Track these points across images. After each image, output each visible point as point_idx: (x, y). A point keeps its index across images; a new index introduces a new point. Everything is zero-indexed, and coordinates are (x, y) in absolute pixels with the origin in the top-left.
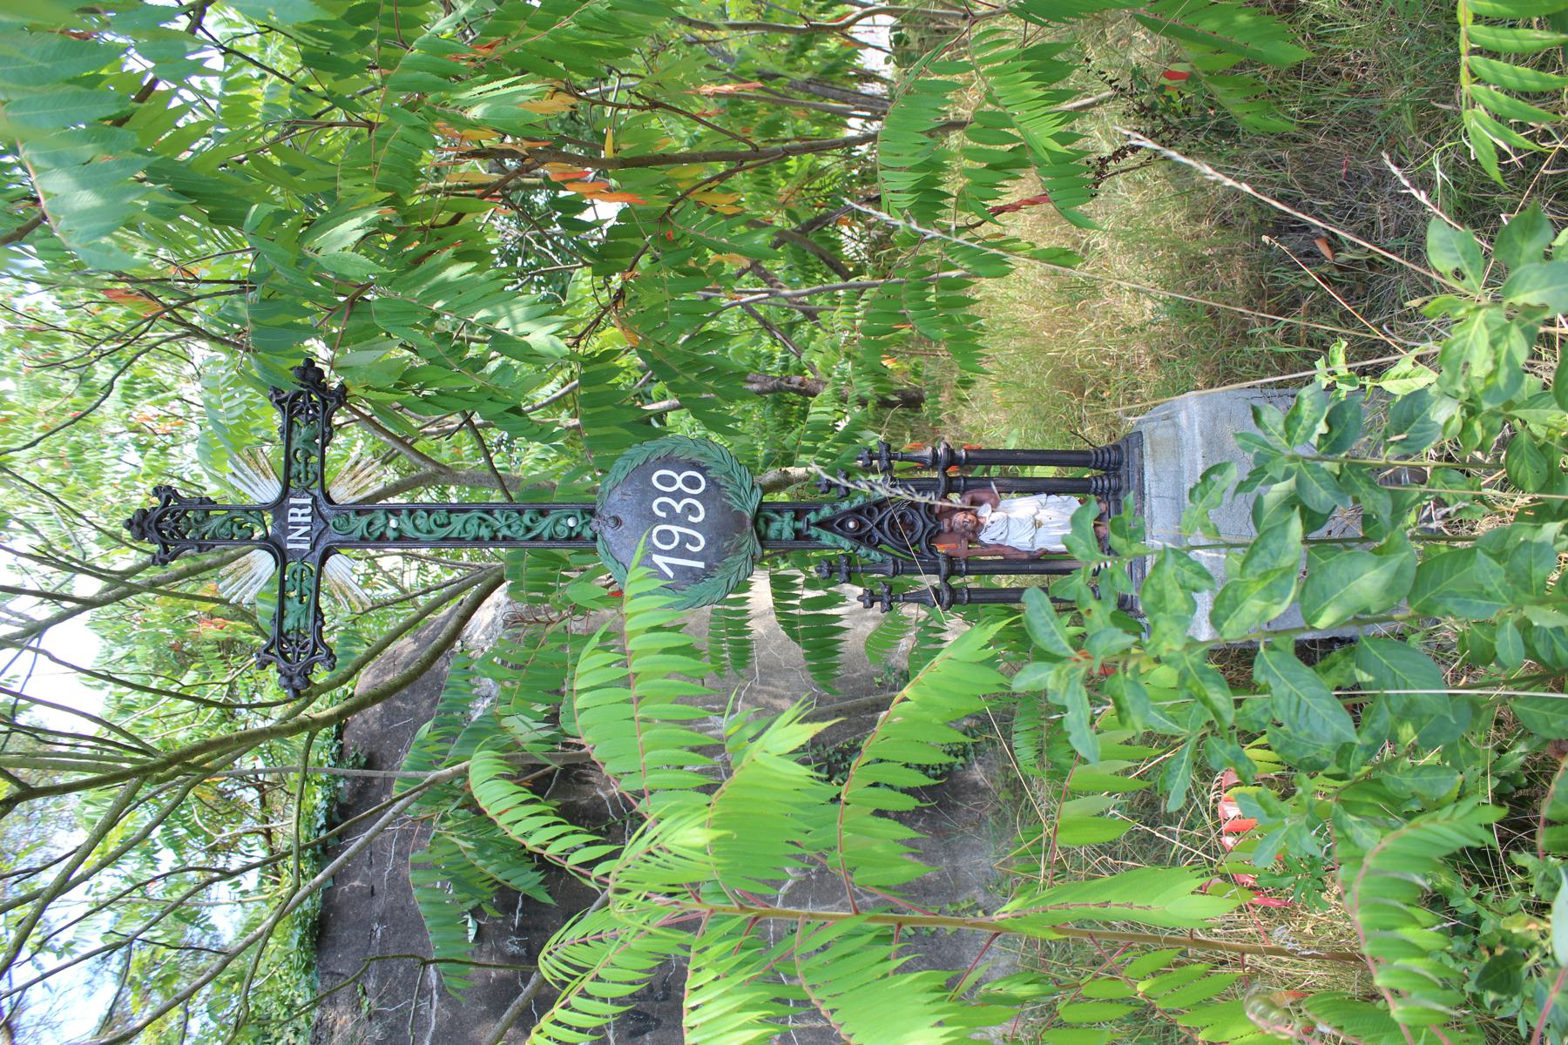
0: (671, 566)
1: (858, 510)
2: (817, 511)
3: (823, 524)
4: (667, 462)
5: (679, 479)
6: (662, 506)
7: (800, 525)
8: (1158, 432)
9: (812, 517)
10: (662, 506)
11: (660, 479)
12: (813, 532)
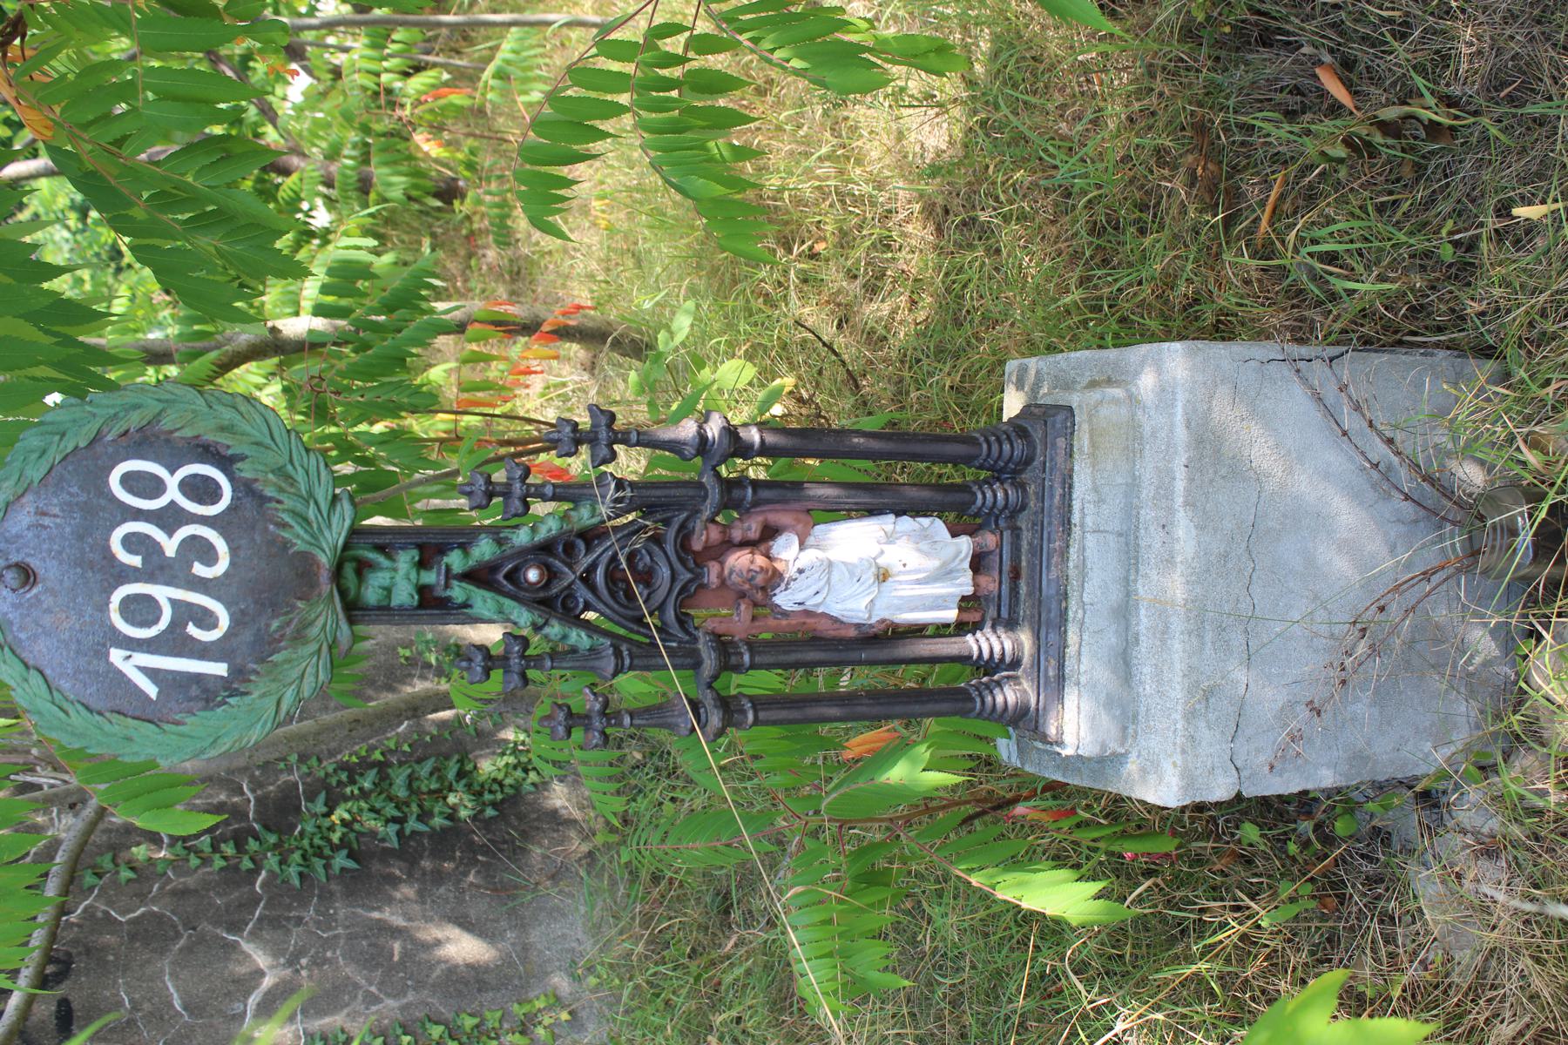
0: (152, 674)
1: (546, 548)
2: (464, 548)
3: (480, 577)
4: (144, 442)
5: (172, 482)
6: (130, 542)
7: (429, 577)
8: (1104, 411)
9: (455, 560)
10: (130, 542)
11: (128, 481)
12: (458, 592)
